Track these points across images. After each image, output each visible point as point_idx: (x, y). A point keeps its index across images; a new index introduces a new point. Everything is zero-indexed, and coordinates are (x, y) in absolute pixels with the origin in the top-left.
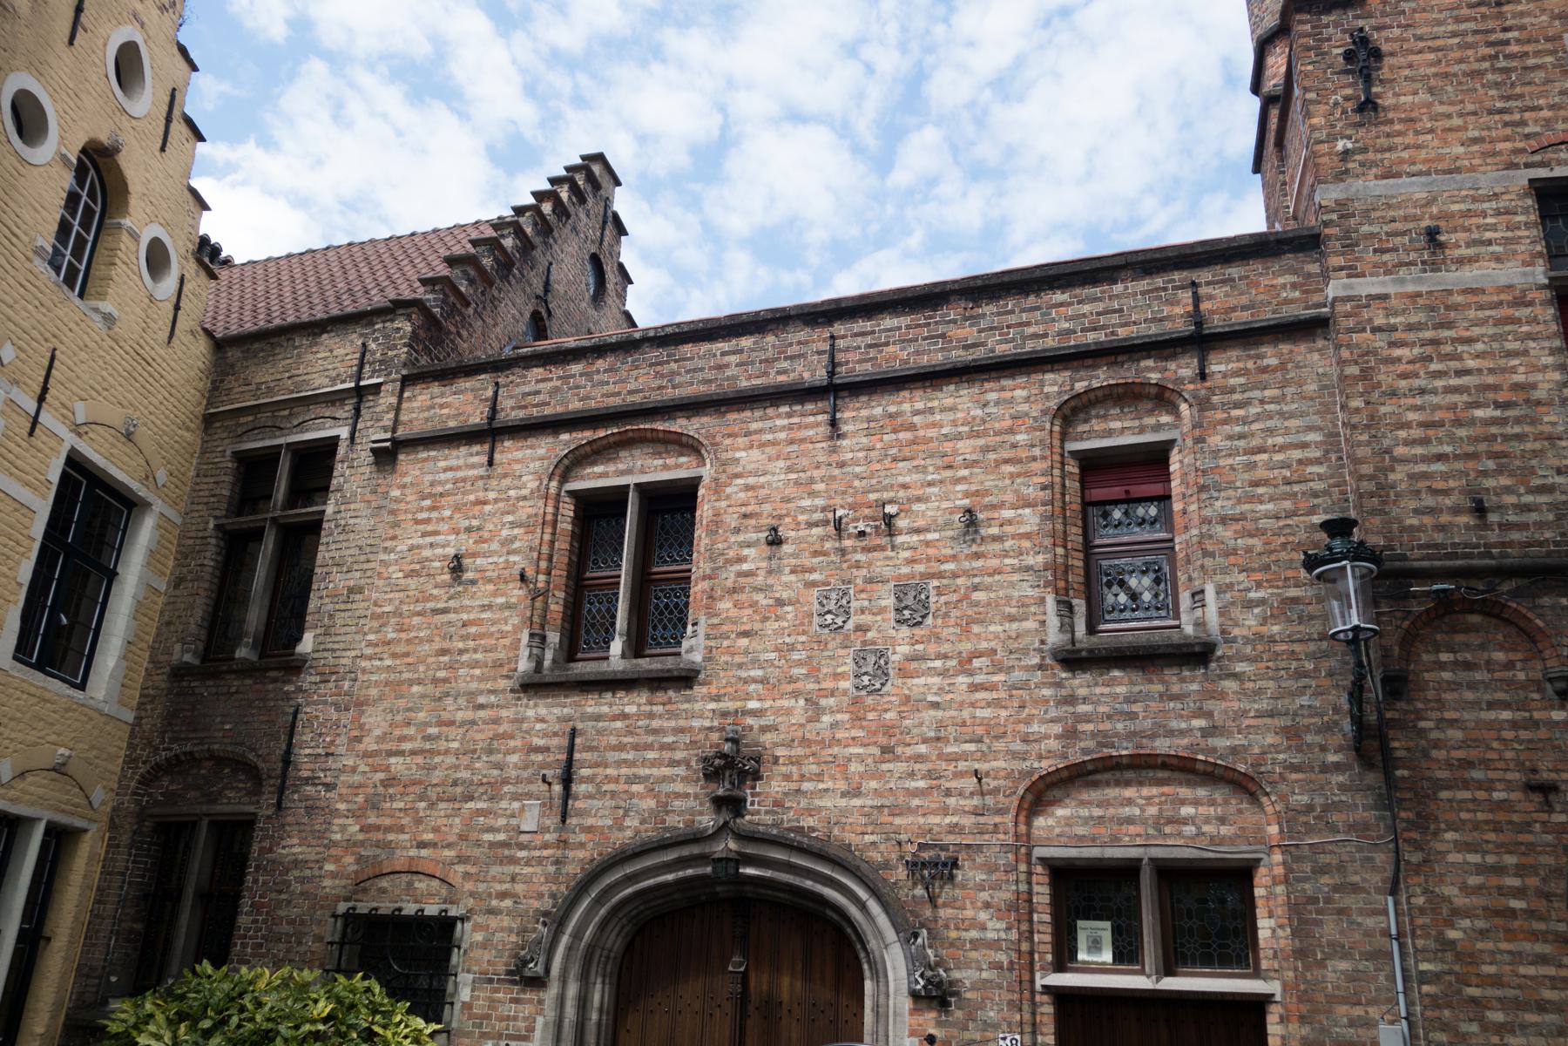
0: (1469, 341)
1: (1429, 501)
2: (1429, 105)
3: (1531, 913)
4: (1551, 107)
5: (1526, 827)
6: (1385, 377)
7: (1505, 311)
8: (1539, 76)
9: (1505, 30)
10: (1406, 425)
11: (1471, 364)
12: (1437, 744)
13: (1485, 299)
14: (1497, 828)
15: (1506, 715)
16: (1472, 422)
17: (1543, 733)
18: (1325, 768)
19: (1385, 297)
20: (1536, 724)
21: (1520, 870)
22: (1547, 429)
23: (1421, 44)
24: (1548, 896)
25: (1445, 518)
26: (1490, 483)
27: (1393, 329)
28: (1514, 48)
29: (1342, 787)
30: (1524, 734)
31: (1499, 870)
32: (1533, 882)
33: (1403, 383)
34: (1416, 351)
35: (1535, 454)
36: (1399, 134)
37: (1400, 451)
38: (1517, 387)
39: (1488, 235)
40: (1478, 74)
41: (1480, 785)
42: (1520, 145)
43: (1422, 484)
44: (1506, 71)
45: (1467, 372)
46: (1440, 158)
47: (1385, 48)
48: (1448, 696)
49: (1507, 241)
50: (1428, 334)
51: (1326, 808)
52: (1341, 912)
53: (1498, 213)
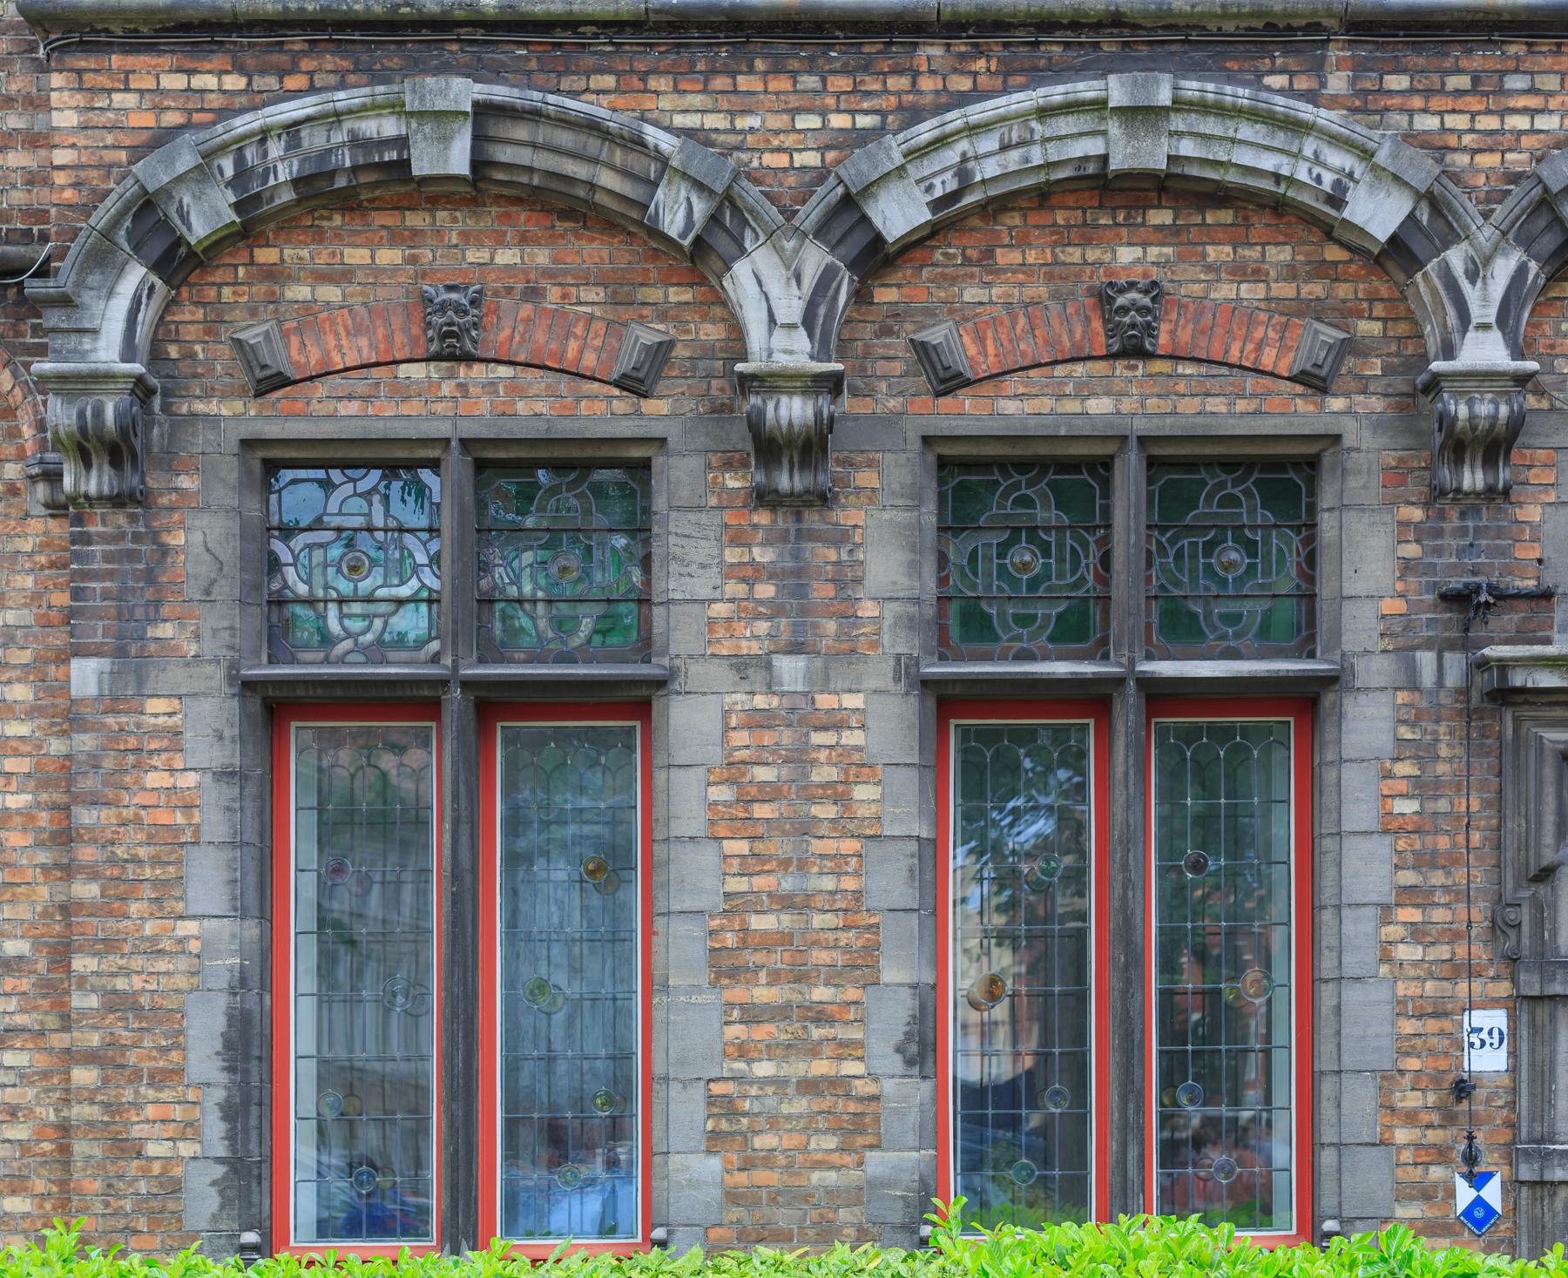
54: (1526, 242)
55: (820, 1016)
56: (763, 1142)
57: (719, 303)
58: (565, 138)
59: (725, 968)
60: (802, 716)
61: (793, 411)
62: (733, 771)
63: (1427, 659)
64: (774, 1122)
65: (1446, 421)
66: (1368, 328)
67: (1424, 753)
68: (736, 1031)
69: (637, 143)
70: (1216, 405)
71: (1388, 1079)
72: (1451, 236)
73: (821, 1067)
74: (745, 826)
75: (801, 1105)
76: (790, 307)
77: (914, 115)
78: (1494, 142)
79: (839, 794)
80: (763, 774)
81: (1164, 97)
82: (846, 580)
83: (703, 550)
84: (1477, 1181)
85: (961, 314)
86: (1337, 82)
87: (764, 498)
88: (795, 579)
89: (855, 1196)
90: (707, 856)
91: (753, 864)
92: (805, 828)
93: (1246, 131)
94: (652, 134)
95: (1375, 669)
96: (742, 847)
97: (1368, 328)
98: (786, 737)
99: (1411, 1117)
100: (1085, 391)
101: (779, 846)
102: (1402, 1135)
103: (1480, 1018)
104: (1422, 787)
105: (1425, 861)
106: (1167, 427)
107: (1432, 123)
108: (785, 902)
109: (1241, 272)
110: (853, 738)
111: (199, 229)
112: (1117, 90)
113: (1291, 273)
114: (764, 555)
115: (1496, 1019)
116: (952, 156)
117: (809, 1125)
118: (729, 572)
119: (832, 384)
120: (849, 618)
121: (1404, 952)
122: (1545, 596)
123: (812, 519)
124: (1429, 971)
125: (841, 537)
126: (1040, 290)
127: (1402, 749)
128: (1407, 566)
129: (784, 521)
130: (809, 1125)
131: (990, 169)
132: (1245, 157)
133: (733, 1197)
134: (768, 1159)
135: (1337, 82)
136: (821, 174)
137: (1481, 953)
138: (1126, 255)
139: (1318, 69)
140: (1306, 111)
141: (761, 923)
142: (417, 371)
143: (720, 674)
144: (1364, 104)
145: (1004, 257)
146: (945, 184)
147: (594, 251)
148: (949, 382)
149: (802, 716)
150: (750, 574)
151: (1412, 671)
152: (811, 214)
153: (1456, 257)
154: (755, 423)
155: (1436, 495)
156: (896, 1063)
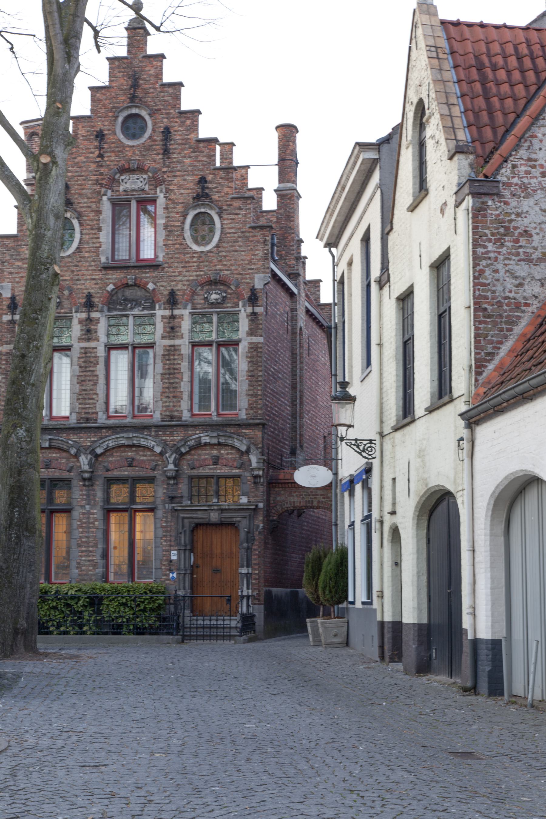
54: (176, 453)
55: (90, 552)
56: (84, 568)
57: (78, 461)
58: (60, 442)
59: (79, 546)
60: (89, 513)
61: (86, 475)
63: (167, 505)
64: (85, 565)
65: (167, 476)
66: (160, 462)
67: (166, 517)
68: (80, 554)
69: (68, 443)
71: (161, 560)
72: (167, 453)
73: (90, 558)
74: (81, 527)
75: (88, 563)
76: (86, 463)
77: (101, 438)
78: (172, 440)
79: (93, 523)
80: (84, 521)
81: (131, 436)
82: (95, 496)
83: (77, 492)
84: (173, 573)
85: (109, 462)
86: (153, 433)
87: (84, 485)
88: (88, 495)
89: (94, 575)
90: (77, 531)
91: (82, 532)
92: (89, 527)
93: (142, 440)
94: (70, 442)
95: (160, 507)
96: (81, 530)
97: (160, 462)
98: (87, 516)
99: (164, 565)
100: (124, 471)
101: (86, 530)
102: (163, 567)
103: (172, 552)
104: (166, 522)
105: (166, 531)
106: (134, 476)
108: (86, 537)
109: (144, 456)
110: (95, 516)
112: (125, 435)
113: (150, 456)
114: (84, 493)
115: (175, 552)
116: (106, 443)
117: (89, 566)
118: (81, 495)
119: (92, 472)
120: (95, 500)
121: (164, 543)
122: (182, 497)
123: (90, 488)
124: (167, 546)
125: (94, 490)
126: (119, 458)
127: (164, 517)
128: (164, 493)
129: (87, 488)
130: (89, 566)
131: (111, 445)
132: (142, 443)
133: (80, 575)
134: (84, 570)
135: (153, 433)
136: (90, 446)
137: (173, 543)
138: (130, 454)
139: (151, 431)
140: (149, 437)
141: (84, 540)
142: (43, 470)
144: (157, 436)
145: (115, 454)
146: (105, 447)
147: (64, 454)
148: (108, 470)
149: (89, 513)
150: (83, 495)
151: (165, 507)
152: (88, 452)
153: (167, 455)
154: (82, 476)
155: (168, 484)
156: (100, 558)
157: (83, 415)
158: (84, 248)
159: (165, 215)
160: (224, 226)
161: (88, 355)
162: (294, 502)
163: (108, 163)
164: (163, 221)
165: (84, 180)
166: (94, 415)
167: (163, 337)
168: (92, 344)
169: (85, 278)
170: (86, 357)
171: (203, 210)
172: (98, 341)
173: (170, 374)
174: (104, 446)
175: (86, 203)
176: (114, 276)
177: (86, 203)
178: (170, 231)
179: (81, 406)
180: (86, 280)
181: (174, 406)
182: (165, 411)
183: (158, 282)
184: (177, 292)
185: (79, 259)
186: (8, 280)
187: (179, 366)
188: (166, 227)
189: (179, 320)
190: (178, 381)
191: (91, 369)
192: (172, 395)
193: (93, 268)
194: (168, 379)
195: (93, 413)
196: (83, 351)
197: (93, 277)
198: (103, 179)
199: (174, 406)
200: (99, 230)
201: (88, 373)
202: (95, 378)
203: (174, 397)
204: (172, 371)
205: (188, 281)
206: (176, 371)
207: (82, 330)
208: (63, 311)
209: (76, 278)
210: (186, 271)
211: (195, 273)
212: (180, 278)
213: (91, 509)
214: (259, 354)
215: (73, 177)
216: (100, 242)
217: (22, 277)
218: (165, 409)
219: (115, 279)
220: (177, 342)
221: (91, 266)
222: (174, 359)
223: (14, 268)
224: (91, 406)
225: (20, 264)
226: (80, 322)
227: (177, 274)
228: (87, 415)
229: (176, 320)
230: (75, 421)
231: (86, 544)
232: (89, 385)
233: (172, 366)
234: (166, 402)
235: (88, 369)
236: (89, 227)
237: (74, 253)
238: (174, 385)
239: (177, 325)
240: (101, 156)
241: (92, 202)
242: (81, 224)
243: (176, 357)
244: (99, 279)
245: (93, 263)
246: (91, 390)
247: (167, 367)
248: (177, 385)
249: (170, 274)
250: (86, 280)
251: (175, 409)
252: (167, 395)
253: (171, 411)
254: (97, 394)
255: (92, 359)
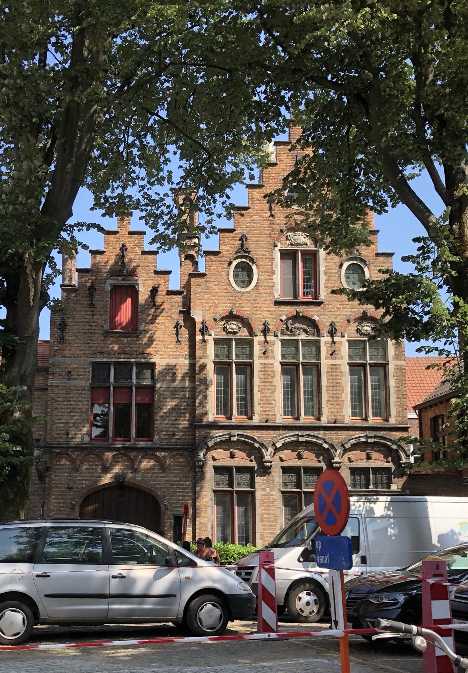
0: (73, 398)
1: (59, 432)
2: (74, 340)
3: (64, 510)
4: (98, 344)
5: (66, 495)
6: (55, 405)
7: (80, 391)
8: (97, 335)
9: (93, 322)
10: (58, 416)
11: (72, 403)
12: (54, 480)
13: (77, 388)
14: (61, 495)
15: (67, 474)
16: (70, 416)
17: (72, 478)
18: (35, 484)
19: (58, 386)
20: (71, 476)
21: (64, 503)
22: (83, 418)
23: (76, 324)
24: (67, 507)
25: (61, 436)
26: (71, 429)
27: (59, 394)
28: (93, 327)
29: (37, 488)
30: (69, 478)
31: (60, 503)
32: (65, 505)
33: (59, 406)
34: (63, 399)
35: (80, 423)
36: (67, 347)
37: (56, 421)
38: (79, 408)
39: (81, 373)
40: (85, 333)
41: (60, 487)
42: (91, 352)
43: (58, 429)
44: (91, 333)
45: (71, 405)
46: (75, 354)
47: (68, 323)
48: (57, 471)
49: (84, 375)
50: (65, 396)
51: (34, 492)
52: (34, 511)
53: (83, 368)
59: (262, 521)
62: (262, 500)
70: (310, 463)
78: (337, 439)
79: (273, 503)
82: (273, 480)
91: (264, 510)
92: (270, 506)
101: (267, 508)
107: (330, 437)
108: (268, 514)
111: (210, 445)
120: (273, 484)
131: (287, 441)
143: (261, 490)
146: (283, 442)
157: (264, 417)
158: (261, 286)
159: (325, 264)
160: (372, 275)
161: (267, 369)
162: (422, 489)
163: (279, 222)
164: (324, 269)
165: (259, 234)
166: (273, 417)
167: (327, 358)
168: (269, 361)
169: (262, 309)
170: (265, 371)
171: (355, 262)
172: (275, 359)
173: (333, 387)
174: (282, 441)
175: (261, 251)
176: (286, 309)
177: (261, 251)
178: (329, 277)
179: (262, 409)
180: (264, 311)
181: (338, 412)
182: (331, 416)
183: (321, 315)
184: (336, 324)
185: (257, 295)
186: (200, 308)
187: (340, 381)
188: (326, 274)
189: (339, 345)
190: (340, 392)
191: (270, 380)
192: (336, 403)
193: (269, 302)
194: (332, 391)
195: (272, 415)
196: (262, 366)
197: (269, 309)
198: (275, 234)
199: (338, 412)
200: (273, 273)
201: (267, 384)
202: (273, 387)
203: (337, 405)
204: (335, 384)
205: (345, 315)
206: (338, 385)
207: (261, 350)
208: (244, 334)
209: (255, 309)
210: (343, 308)
211: (350, 310)
212: (338, 313)
213: (271, 491)
214: (404, 374)
215: (250, 231)
216: (274, 283)
217: (211, 306)
218: (330, 414)
219: (287, 311)
220: (337, 362)
221: (267, 300)
222: (336, 376)
223: (205, 299)
224: (271, 409)
225: (209, 296)
226: (259, 343)
227: (336, 310)
228: (267, 417)
229: (336, 345)
230: (258, 421)
231: (267, 520)
232: (268, 393)
233: (334, 381)
234: (331, 408)
235: (267, 380)
236: (265, 270)
237: (253, 290)
238: (338, 395)
239: (337, 349)
240: (272, 216)
241: (266, 251)
242: (258, 268)
243: (338, 374)
244: (274, 311)
245: (268, 298)
246: (270, 397)
247: (331, 381)
248: (339, 396)
249: (330, 309)
250: (264, 311)
251: (338, 414)
252: (331, 403)
253: (336, 416)
254: (275, 400)
255: (270, 373)
